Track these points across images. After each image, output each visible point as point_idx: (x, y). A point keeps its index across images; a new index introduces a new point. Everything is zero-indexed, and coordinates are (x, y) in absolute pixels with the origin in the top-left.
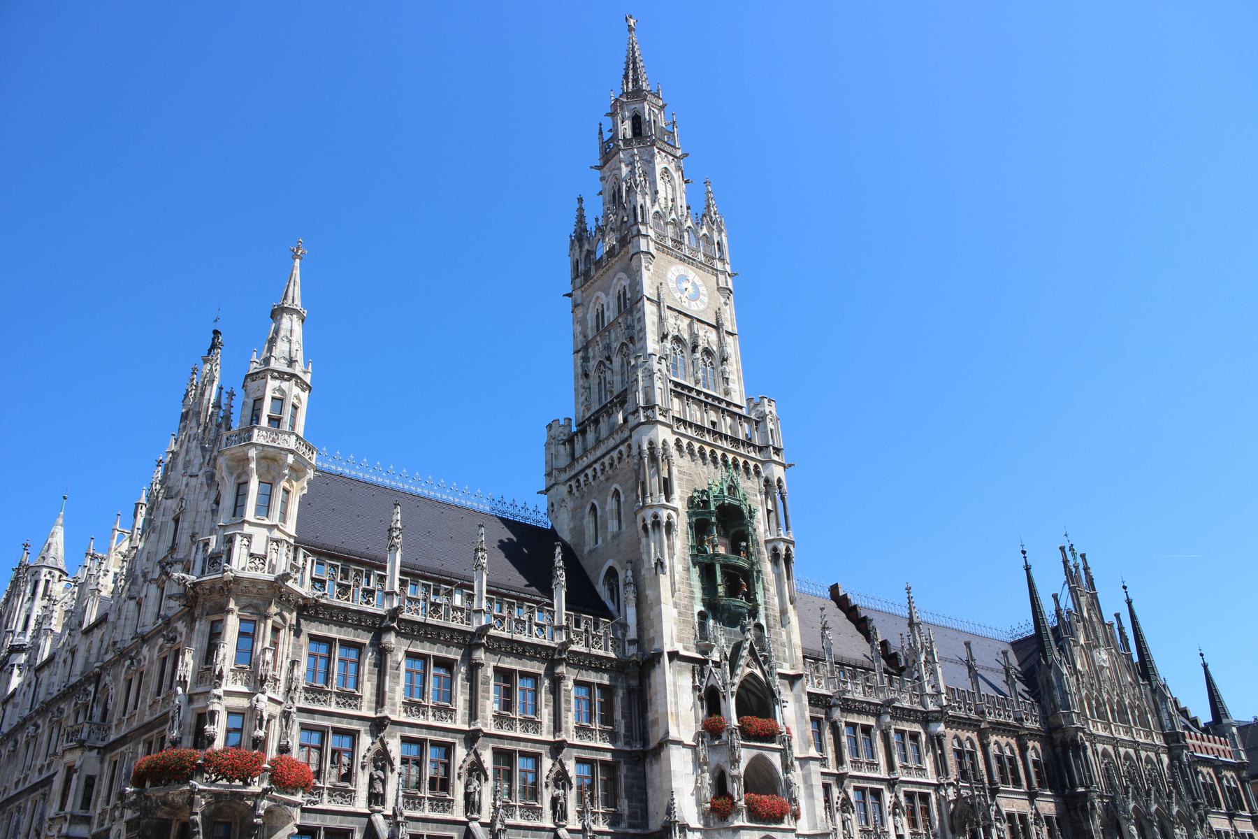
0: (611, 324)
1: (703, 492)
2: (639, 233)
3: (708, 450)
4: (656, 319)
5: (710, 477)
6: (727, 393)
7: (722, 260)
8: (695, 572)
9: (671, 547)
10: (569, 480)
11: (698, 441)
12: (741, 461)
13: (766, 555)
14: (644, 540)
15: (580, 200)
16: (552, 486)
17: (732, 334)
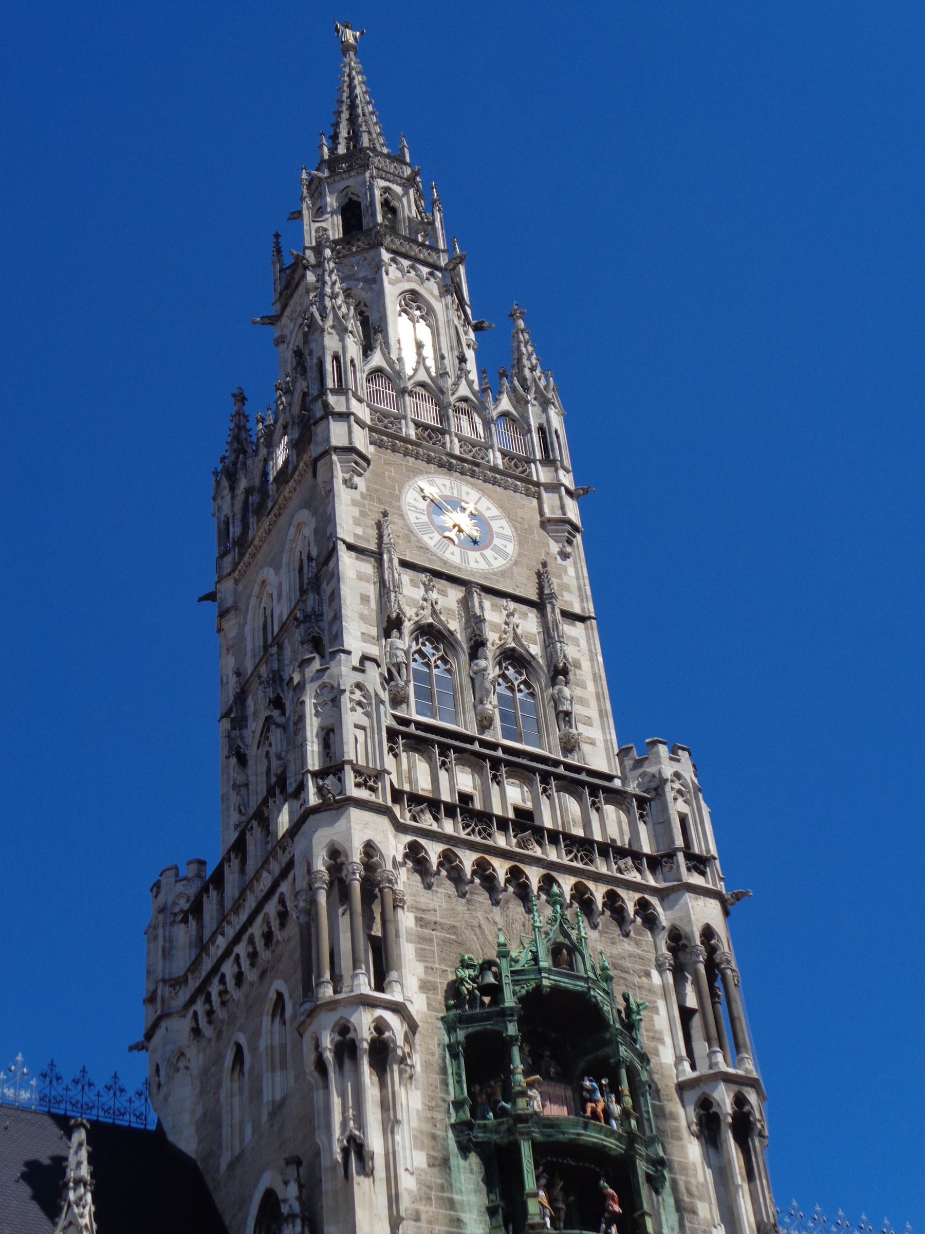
0: (283, 627)
1: (487, 965)
2: (329, 413)
3: (501, 868)
4: (371, 591)
5: (509, 933)
6: (569, 746)
7: (548, 461)
8: (468, 1176)
9: (387, 1106)
10: (192, 1001)
11: (472, 846)
12: (598, 892)
13: (683, 1116)
14: (319, 1095)
15: (241, 398)
16: (159, 1019)
17: (582, 619)
